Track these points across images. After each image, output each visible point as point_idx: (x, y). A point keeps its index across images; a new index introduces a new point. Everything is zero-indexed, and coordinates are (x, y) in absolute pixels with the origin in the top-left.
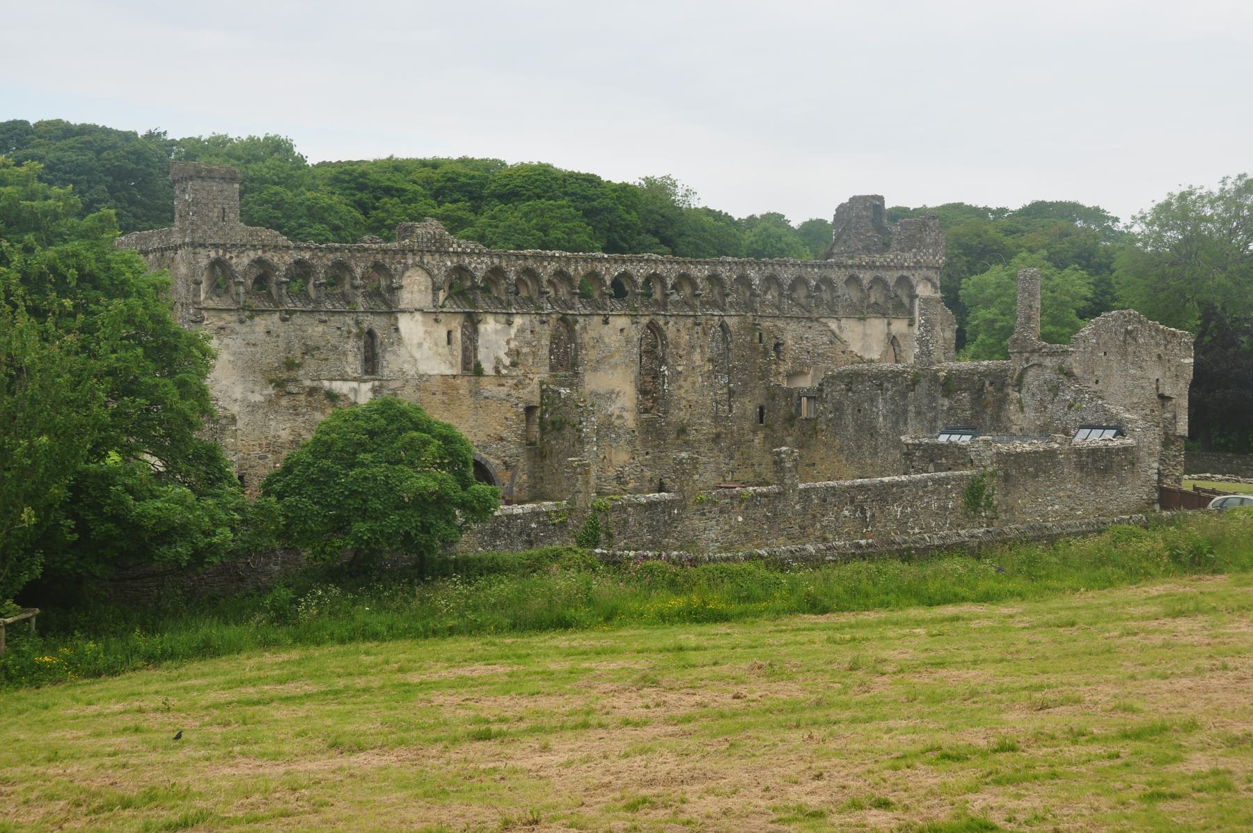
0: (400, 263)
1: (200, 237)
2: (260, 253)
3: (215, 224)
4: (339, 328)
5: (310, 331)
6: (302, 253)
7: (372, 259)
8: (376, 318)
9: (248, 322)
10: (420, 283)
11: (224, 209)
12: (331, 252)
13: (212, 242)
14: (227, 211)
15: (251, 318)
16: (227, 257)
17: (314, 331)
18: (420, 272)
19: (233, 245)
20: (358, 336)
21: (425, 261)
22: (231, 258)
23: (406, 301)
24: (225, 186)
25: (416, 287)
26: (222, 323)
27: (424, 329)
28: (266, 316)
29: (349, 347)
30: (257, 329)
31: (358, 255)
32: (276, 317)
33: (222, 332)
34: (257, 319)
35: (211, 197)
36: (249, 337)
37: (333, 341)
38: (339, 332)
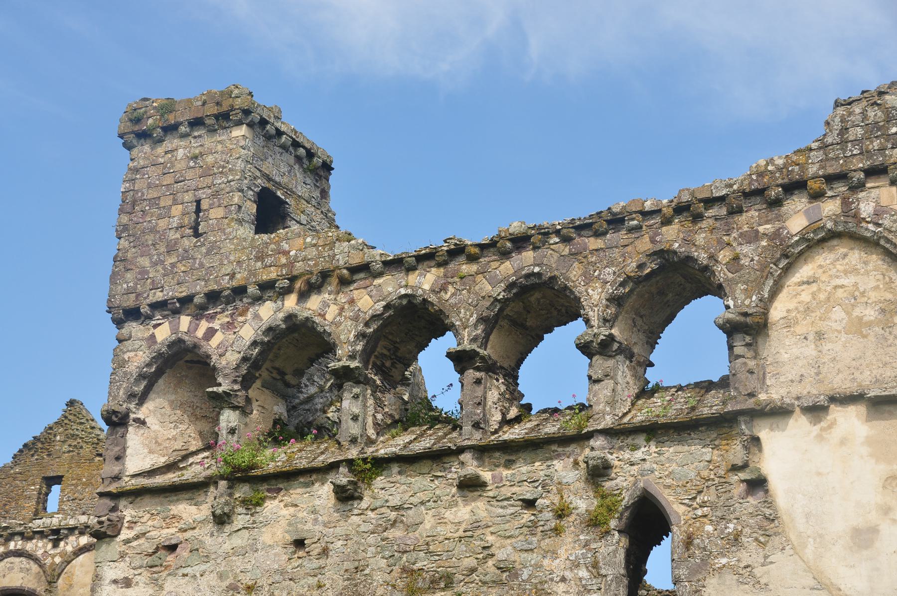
0: (753, 237)
1: (128, 292)
2: (290, 302)
3: (171, 249)
4: (530, 504)
5: (429, 522)
6: (413, 278)
7: (645, 244)
8: (670, 451)
9: (240, 520)
10: (856, 296)
11: (198, 202)
12: (505, 255)
13: (159, 296)
14: (205, 205)
15: (252, 504)
16: (200, 333)
17: (441, 521)
18: (855, 256)
19: (213, 297)
20: (594, 522)
21: (866, 209)
22: (211, 333)
23: (792, 373)
24: (208, 141)
25: (838, 313)
26: (168, 534)
27: (883, 469)
28: (297, 493)
29: (556, 566)
30: (266, 537)
31: (594, 243)
32: (324, 492)
33: (170, 558)
34: (272, 507)
35: (168, 180)
36: (238, 563)
37: (504, 552)
38: (527, 516)
